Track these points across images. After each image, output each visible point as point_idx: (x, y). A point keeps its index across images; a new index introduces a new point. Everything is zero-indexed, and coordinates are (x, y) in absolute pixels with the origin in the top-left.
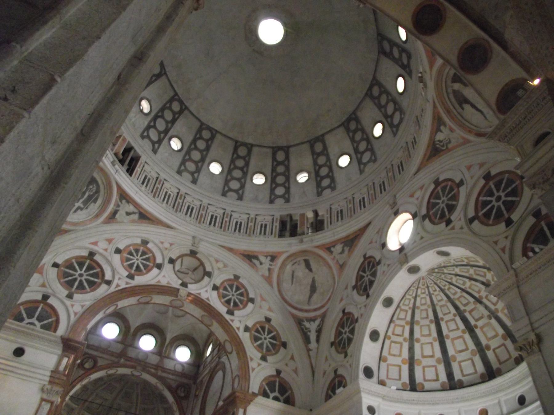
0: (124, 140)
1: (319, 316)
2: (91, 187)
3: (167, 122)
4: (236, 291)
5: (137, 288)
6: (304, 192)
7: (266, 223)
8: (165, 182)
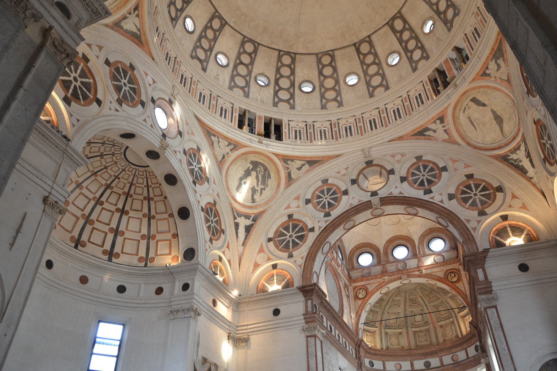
0: (260, 117)
1: (519, 142)
2: (259, 169)
3: (288, 77)
4: (424, 171)
5: (336, 220)
6: (438, 38)
7: (419, 93)
8: (314, 124)
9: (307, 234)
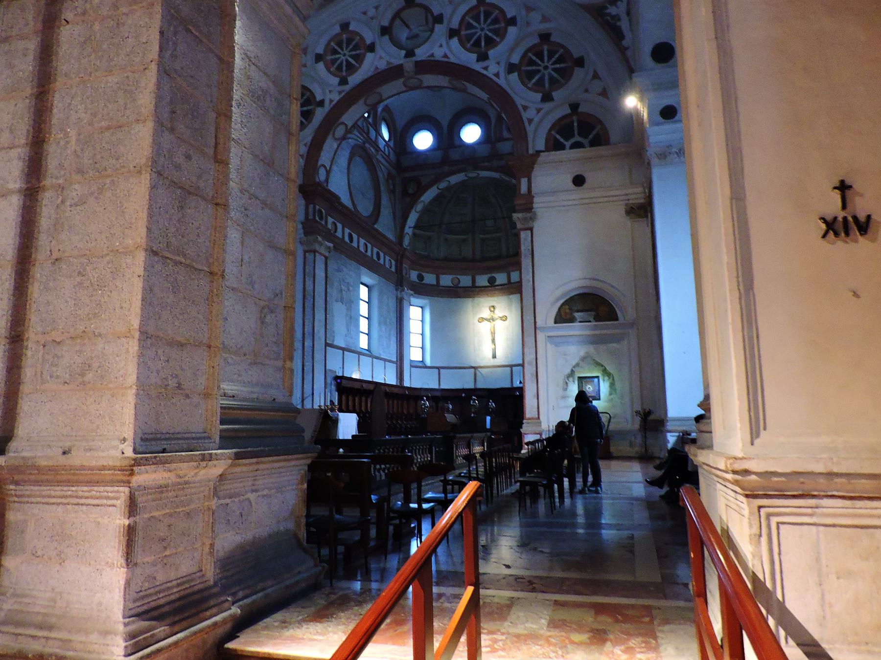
4: (485, 21)
9: (314, 109)
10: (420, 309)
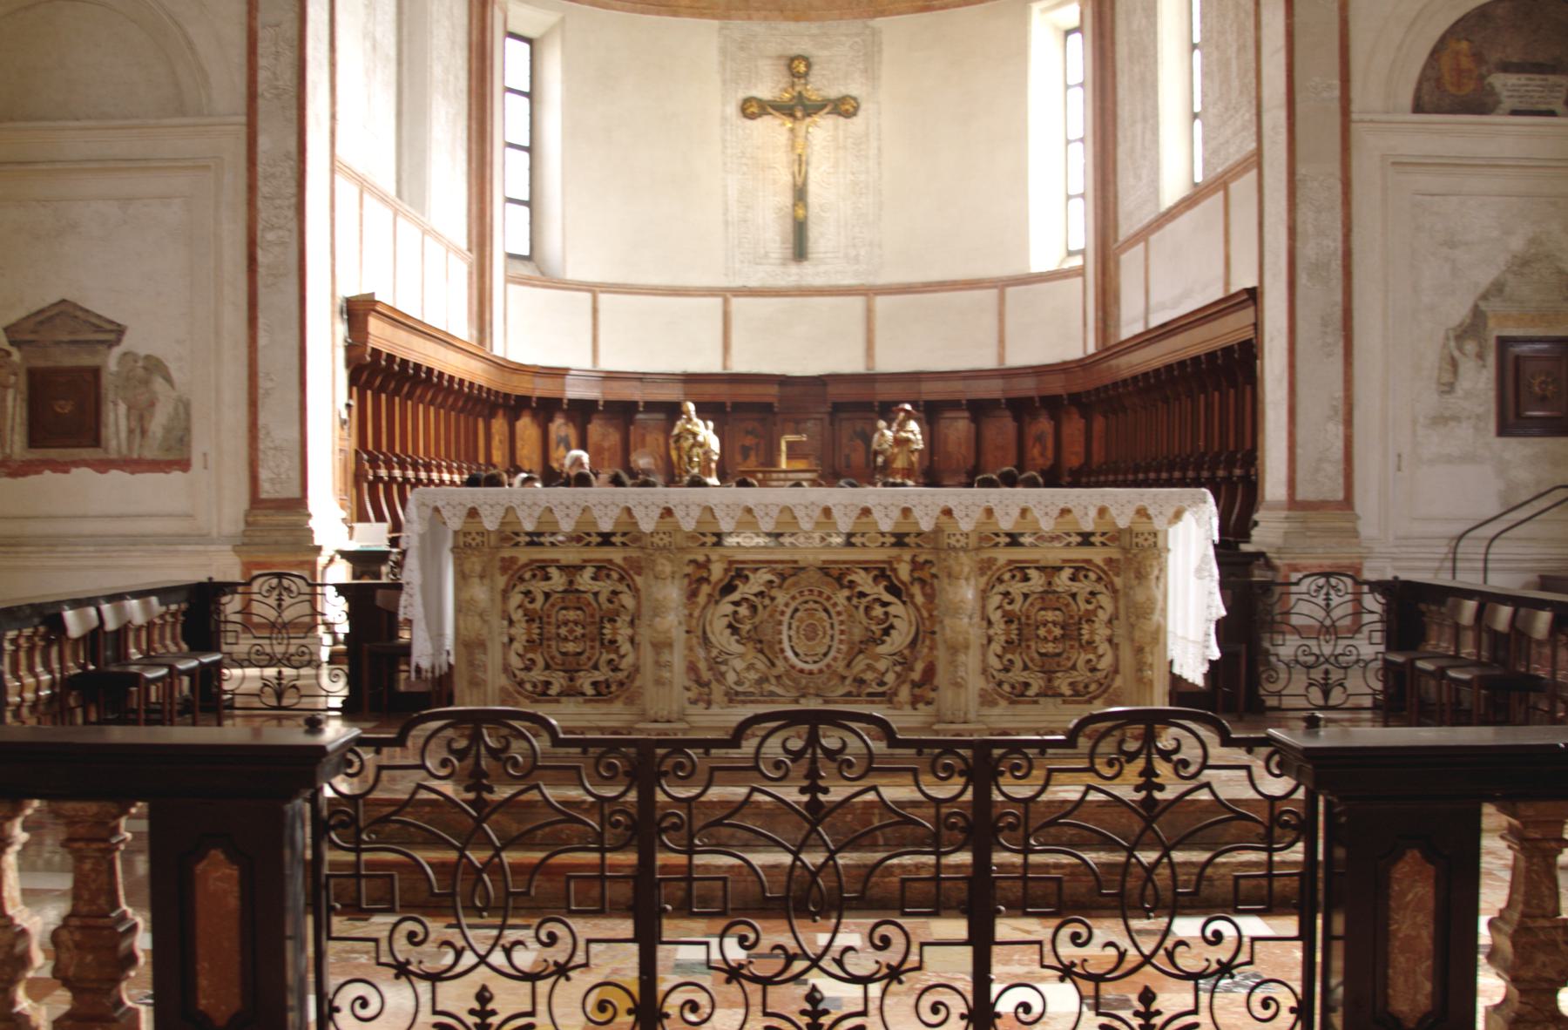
10: (526, 47)
